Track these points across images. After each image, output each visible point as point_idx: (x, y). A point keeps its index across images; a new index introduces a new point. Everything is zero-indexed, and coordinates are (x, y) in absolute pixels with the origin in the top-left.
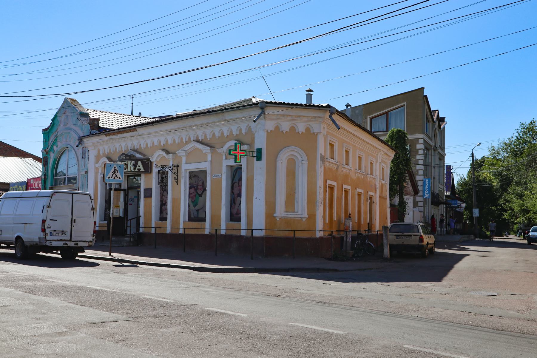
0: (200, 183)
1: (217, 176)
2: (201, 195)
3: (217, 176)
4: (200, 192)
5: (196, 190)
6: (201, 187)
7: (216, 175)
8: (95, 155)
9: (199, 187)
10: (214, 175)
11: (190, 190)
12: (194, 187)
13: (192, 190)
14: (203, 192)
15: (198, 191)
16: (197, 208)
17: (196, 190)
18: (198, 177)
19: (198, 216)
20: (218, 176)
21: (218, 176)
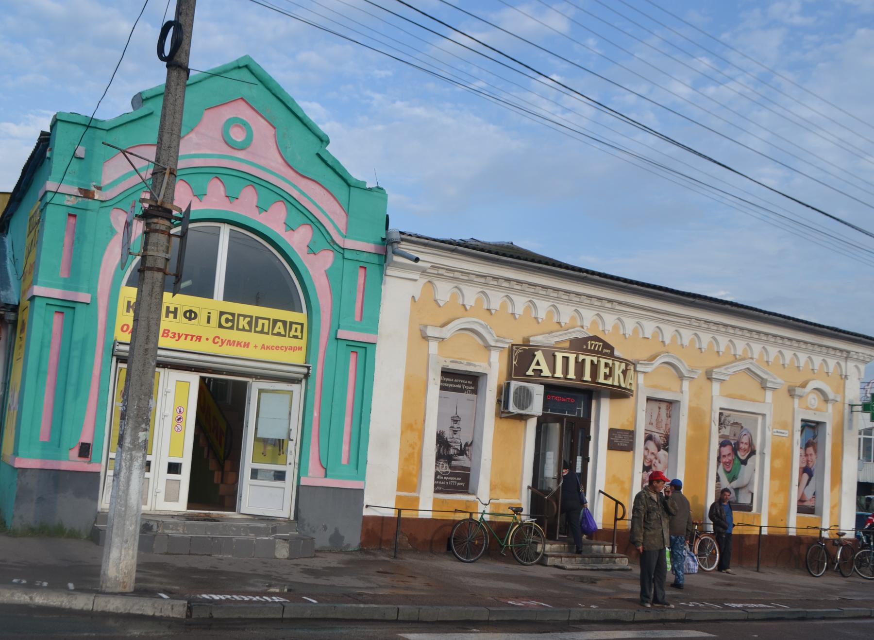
0: (745, 439)
1: (781, 433)
2: (744, 462)
3: (781, 433)
4: (742, 455)
5: (736, 449)
6: (746, 447)
7: (779, 431)
8: (413, 297)
9: (742, 446)
10: (775, 430)
11: (722, 448)
12: (731, 444)
13: (727, 450)
14: (749, 457)
15: (739, 453)
16: (735, 484)
17: (736, 449)
18: (742, 427)
19: (737, 500)
20: (783, 433)
21: (783, 433)
